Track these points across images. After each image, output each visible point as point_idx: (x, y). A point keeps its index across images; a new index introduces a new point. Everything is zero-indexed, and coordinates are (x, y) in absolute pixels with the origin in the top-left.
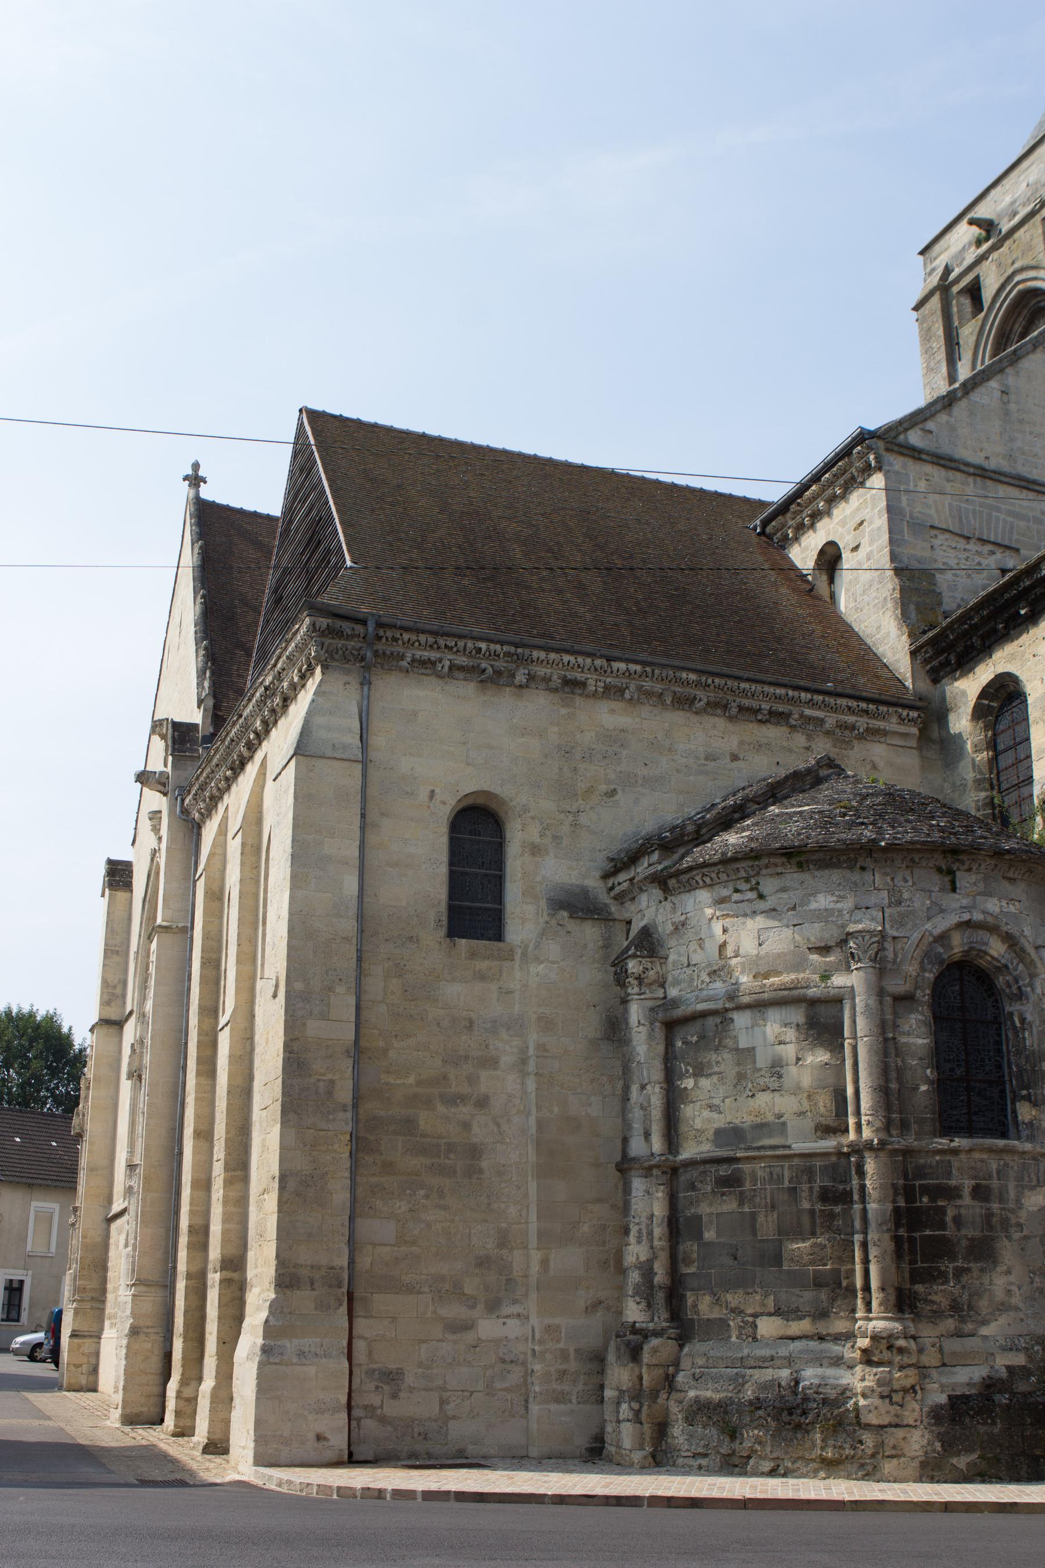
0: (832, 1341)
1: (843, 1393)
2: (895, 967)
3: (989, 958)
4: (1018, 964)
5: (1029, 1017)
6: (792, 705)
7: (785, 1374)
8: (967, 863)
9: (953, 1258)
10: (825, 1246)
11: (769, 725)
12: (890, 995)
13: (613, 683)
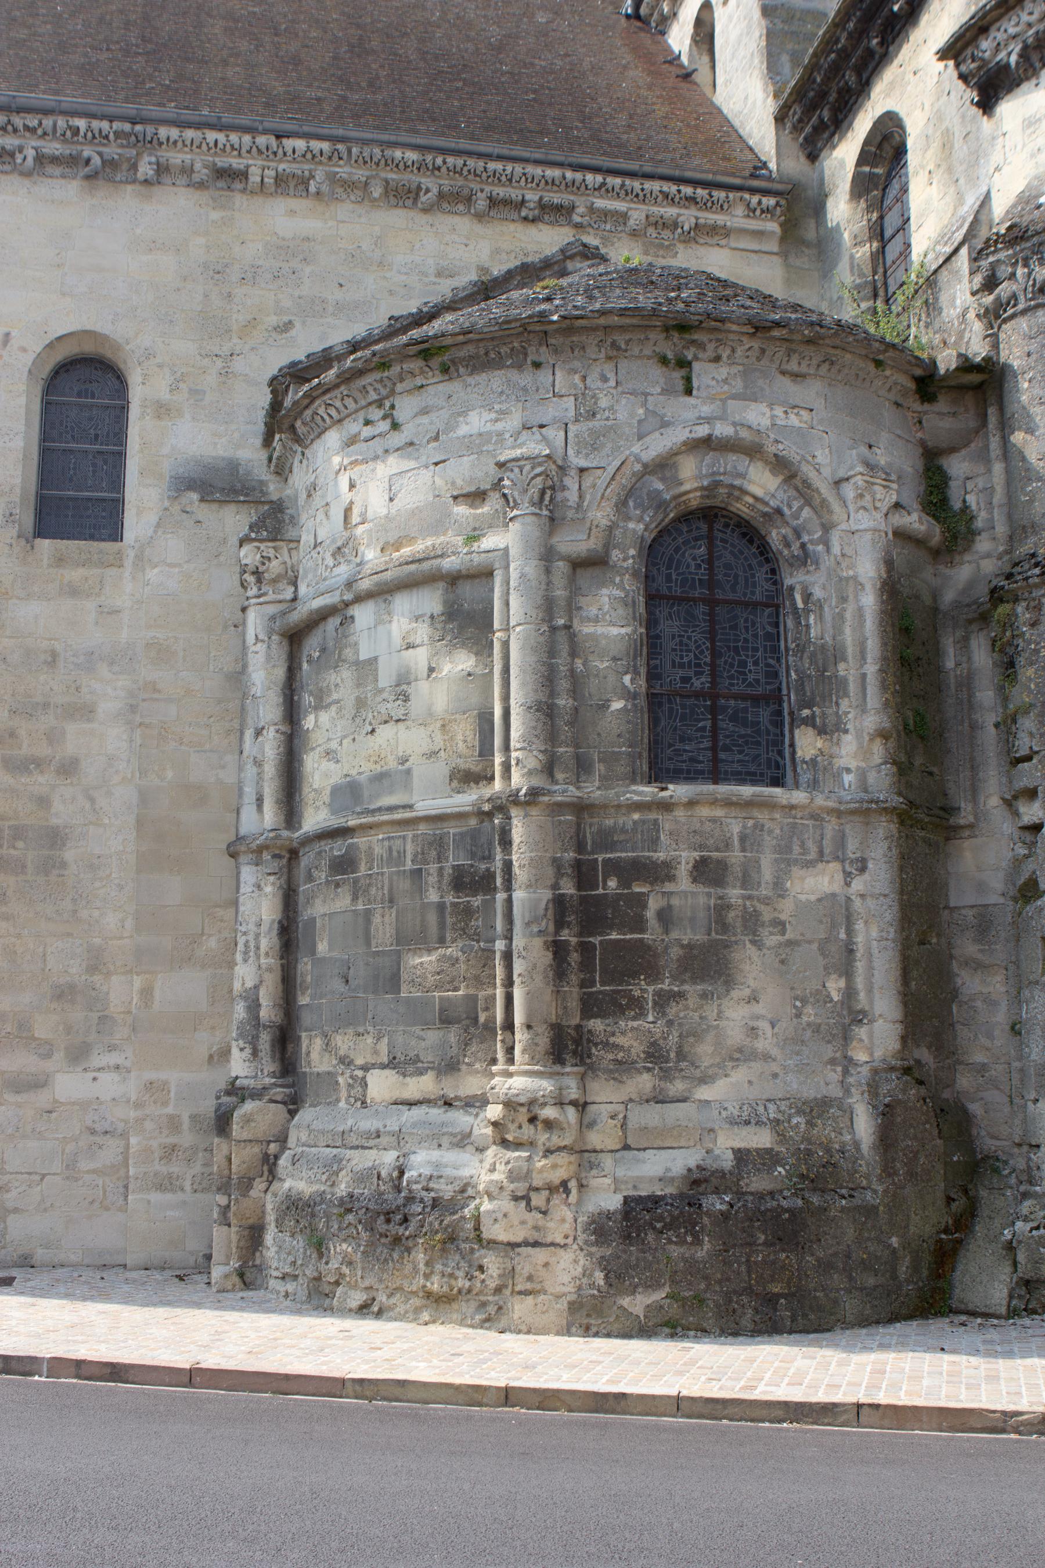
0: (462, 1107)
1: (463, 1191)
2: (580, 516)
3: (750, 500)
4: (801, 509)
5: (818, 593)
6: (572, 193)
8: (710, 347)
9: (653, 974)
10: (457, 959)
11: (541, 226)
12: (563, 558)
13: (288, 171)
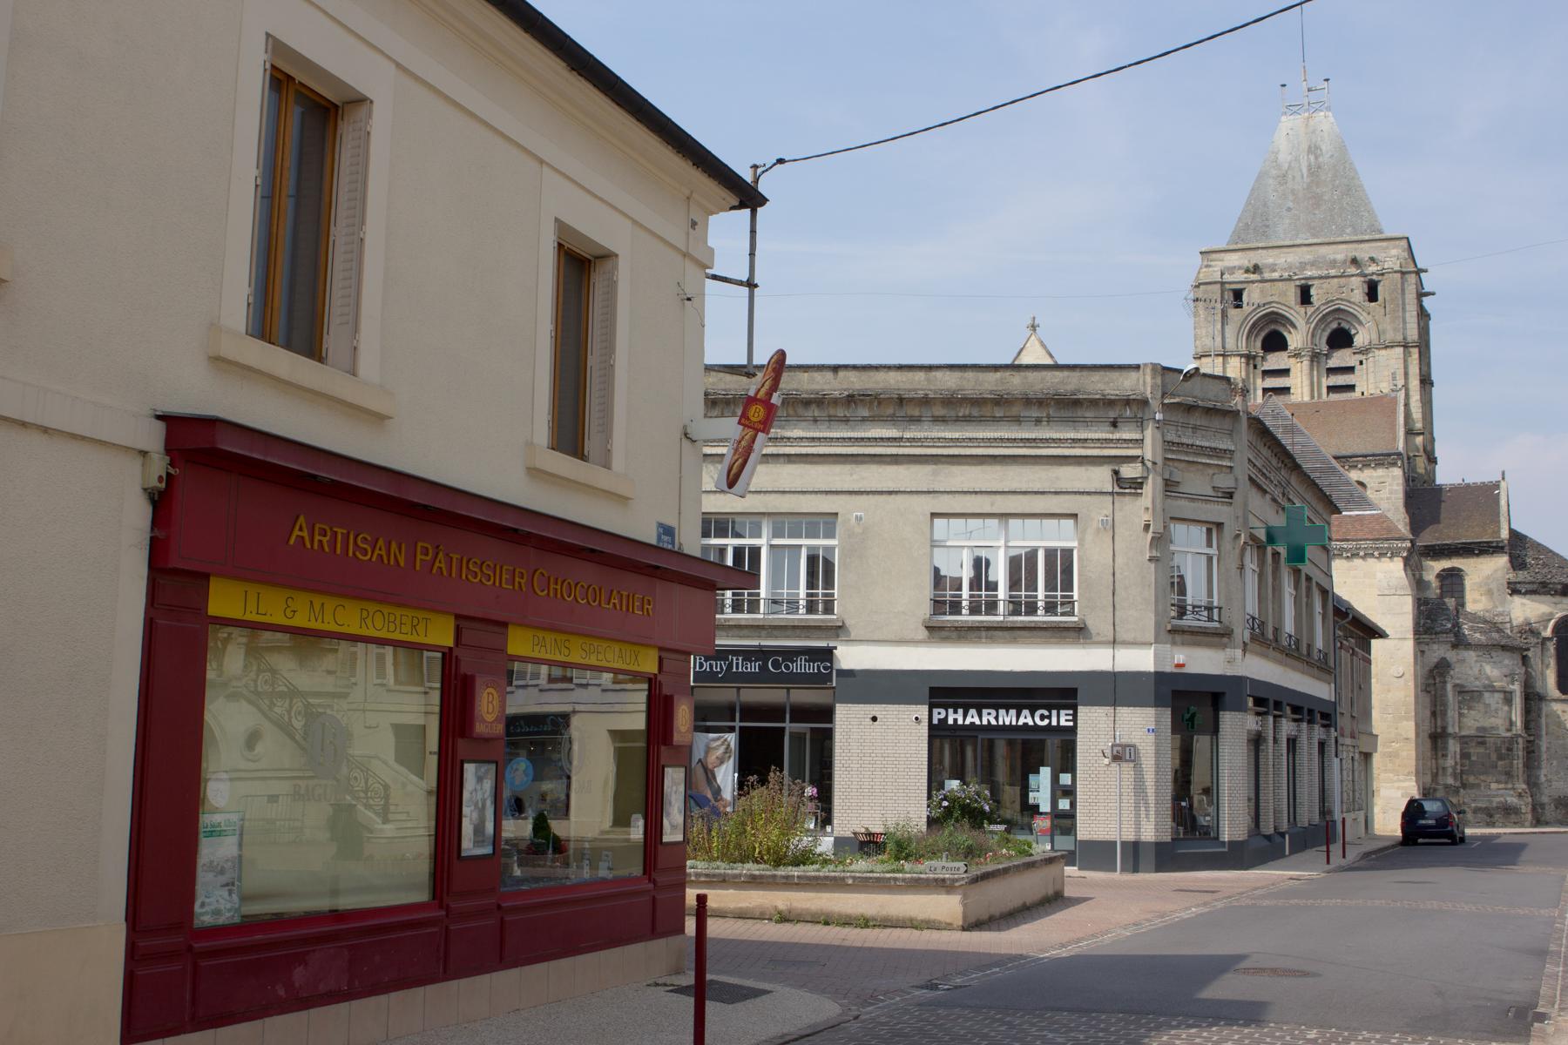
7: (1502, 799)
